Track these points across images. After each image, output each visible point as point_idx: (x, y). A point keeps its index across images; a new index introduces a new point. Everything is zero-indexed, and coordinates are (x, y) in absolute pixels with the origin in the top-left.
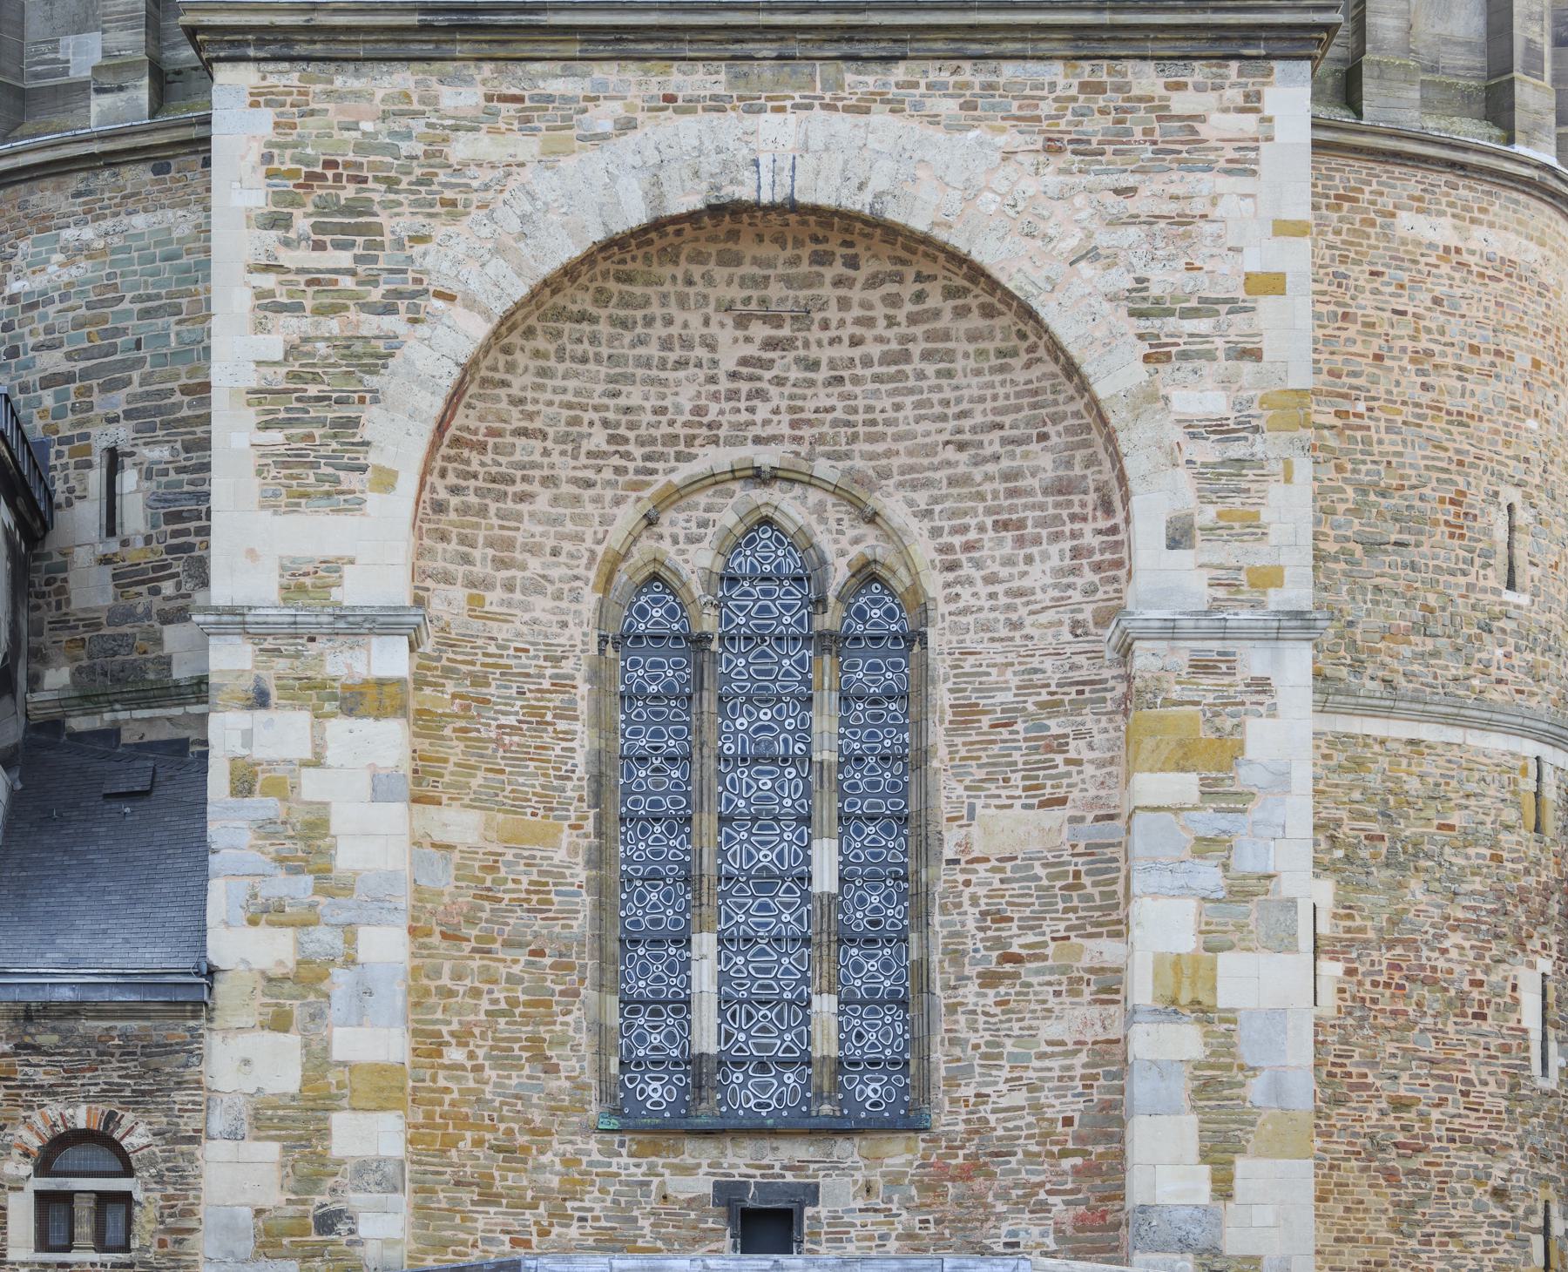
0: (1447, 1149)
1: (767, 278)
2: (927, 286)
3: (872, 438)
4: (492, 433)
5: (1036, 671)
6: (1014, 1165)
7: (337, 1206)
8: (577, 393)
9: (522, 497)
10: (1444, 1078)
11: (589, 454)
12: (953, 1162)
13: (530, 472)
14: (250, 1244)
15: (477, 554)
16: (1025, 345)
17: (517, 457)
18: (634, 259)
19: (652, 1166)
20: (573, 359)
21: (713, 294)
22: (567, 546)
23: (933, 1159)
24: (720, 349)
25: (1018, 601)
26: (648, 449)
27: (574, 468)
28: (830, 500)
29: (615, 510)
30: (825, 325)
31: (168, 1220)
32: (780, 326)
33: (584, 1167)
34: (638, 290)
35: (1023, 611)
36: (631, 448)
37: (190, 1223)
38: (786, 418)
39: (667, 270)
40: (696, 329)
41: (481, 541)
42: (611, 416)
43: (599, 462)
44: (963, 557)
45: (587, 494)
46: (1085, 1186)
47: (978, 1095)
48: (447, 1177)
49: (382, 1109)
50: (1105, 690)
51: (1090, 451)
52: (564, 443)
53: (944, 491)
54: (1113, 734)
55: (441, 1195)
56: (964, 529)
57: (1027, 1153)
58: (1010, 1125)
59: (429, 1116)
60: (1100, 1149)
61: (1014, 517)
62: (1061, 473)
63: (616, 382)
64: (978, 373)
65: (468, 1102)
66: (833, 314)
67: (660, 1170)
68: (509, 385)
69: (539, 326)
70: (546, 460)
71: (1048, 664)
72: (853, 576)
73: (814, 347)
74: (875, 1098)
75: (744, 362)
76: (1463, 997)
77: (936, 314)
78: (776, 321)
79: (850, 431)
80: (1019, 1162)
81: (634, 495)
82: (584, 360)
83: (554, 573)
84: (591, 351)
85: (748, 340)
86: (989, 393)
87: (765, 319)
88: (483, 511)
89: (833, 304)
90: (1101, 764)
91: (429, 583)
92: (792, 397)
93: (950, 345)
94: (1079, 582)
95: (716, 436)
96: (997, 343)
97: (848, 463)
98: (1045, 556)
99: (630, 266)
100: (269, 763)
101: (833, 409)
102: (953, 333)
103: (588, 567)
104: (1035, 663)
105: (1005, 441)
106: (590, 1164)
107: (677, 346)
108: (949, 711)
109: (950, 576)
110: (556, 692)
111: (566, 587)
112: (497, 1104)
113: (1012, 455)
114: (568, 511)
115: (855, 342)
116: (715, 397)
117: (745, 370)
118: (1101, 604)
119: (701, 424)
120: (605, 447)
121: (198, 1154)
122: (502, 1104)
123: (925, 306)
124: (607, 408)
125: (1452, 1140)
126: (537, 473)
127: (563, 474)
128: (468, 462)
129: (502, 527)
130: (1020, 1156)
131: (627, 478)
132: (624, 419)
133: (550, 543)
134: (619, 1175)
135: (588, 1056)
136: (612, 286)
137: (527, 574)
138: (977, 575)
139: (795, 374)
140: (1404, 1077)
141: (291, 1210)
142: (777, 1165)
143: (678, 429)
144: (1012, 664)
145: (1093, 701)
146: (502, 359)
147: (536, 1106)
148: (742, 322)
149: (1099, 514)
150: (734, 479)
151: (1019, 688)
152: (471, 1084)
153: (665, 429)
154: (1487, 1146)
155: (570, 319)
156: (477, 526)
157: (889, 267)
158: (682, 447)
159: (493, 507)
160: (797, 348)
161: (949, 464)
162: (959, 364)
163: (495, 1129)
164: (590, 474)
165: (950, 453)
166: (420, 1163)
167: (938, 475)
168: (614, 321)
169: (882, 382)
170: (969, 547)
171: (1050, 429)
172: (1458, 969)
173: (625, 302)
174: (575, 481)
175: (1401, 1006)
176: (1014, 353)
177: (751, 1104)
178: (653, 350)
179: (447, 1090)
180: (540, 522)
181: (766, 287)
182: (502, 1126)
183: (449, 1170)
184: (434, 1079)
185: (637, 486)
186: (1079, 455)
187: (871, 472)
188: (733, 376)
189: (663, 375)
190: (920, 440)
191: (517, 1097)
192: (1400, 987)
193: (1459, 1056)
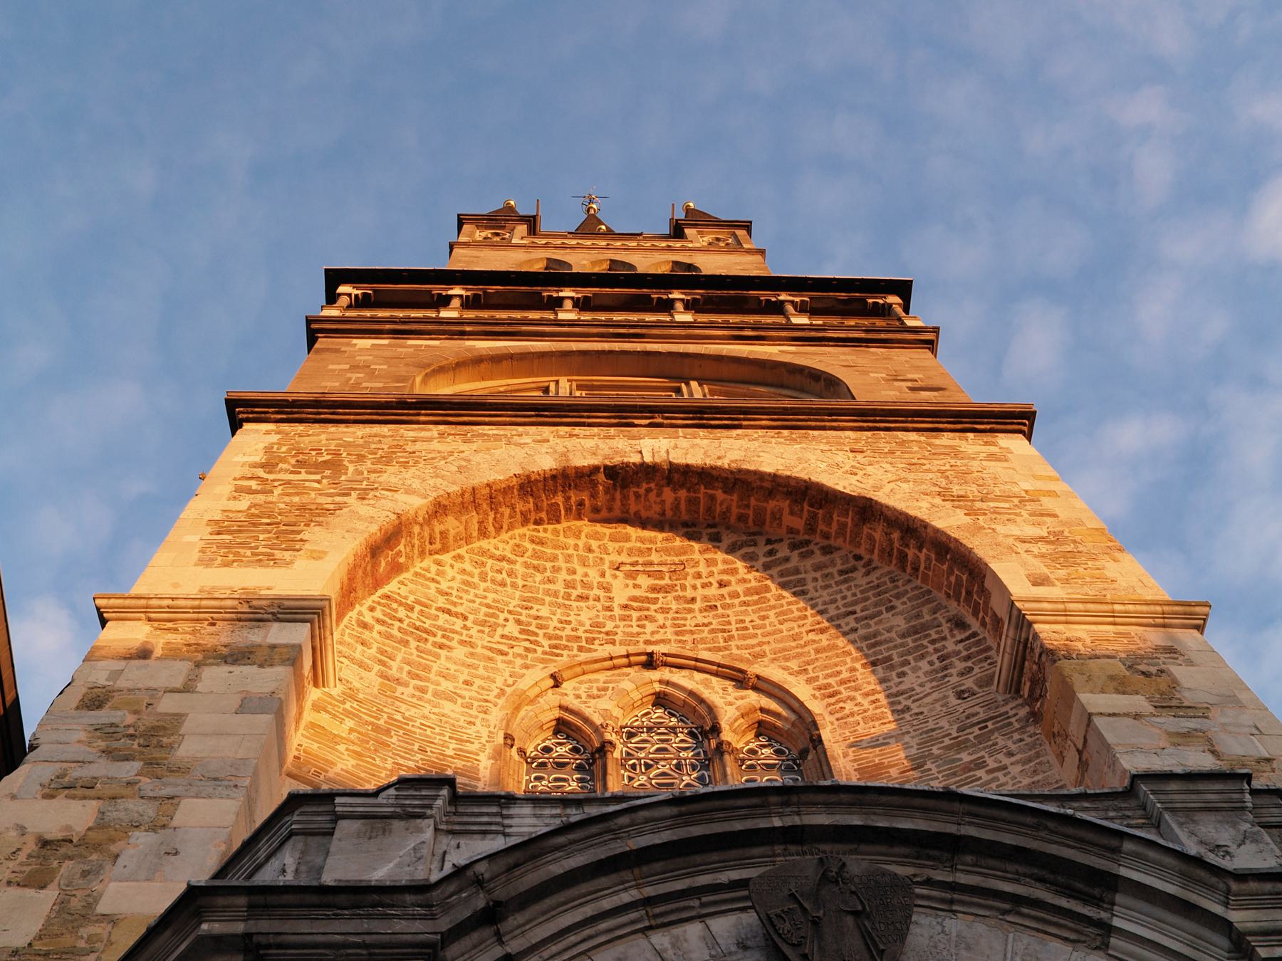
1: (649, 549)
2: (776, 546)
3: (744, 637)
4: (418, 602)
5: (933, 730)
8: (494, 601)
9: (441, 646)
11: (502, 636)
13: (451, 635)
15: (395, 665)
16: (862, 563)
17: (440, 622)
18: (545, 530)
20: (493, 581)
21: (607, 558)
22: (478, 682)
24: (614, 591)
25: (900, 698)
26: (554, 642)
27: (489, 642)
28: (714, 679)
29: (524, 671)
30: (699, 575)
32: (663, 578)
34: (549, 551)
35: (909, 703)
36: (540, 639)
38: (670, 630)
39: (571, 542)
40: (594, 576)
41: (399, 658)
42: (523, 618)
43: (511, 642)
44: (842, 688)
45: (500, 658)
50: (1009, 717)
51: (935, 604)
52: (483, 626)
53: (813, 657)
54: (1029, 740)
56: (839, 673)
61: (880, 657)
62: (912, 623)
63: (529, 601)
64: (826, 587)
66: (702, 568)
68: (438, 582)
69: (467, 556)
70: (465, 632)
71: (944, 723)
72: (743, 716)
73: (689, 589)
75: (634, 599)
77: (787, 559)
78: (659, 574)
79: (725, 635)
81: (542, 666)
82: (503, 584)
83: (467, 694)
84: (508, 581)
85: (635, 586)
86: (838, 597)
87: (649, 574)
88: (406, 643)
89: (702, 563)
90: (1025, 762)
91: (343, 659)
92: (674, 619)
93: (800, 576)
94: (954, 671)
95: (614, 639)
96: (839, 567)
97: (727, 652)
98: (915, 670)
99: (542, 534)
100: (129, 690)
101: (710, 623)
102: (802, 569)
103: (498, 696)
104: (931, 725)
105: (857, 620)
107: (579, 587)
108: (856, 773)
109: (832, 700)
110: (459, 759)
111: (476, 704)
113: (868, 626)
114: (482, 664)
115: (722, 584)
116: (612, 618)
117: (635, 604)
118: (979, 675)
119: (601, 632)
120: (516, 634)
123: (777, 557)
124: (521, 614)
126: (456, 637)
127: (479, 643)
128: (396, 611)
129: (418, 656)
131: (535, 655)
132: (534, 622)
133: (462, 678)
136: (527, 545)
137: (438, 688)
138: (857, 694)
139: (674, 606)
143: (580, 633)
144: (908, 732)
145: (998, 729)
146: (434, 568)
148: (631, 575)
149: (956, 632)
150: (630, 665)
151: (918, 744)
153: (568, 632)
155: (492, 557)
156: (397, 649)
157: (744, 538)
158: (584, 644)
159: (413, 644)
160: (676, 591)
161: (814, 641)
162: (810, 586)
164: (504, 648)
165: (812, 636)
167: (806, 649)
168: (526, 565)
169: (749, 605)
170: (842, 682)
171: (895, 602)
173: (536, 555)
174: (490, 649)
176: (854, 569)
178: (559, 586)
180: (455, 663)
181: (650, 555)
185: (542, 661)
186: (925, 610)
187: (748, 656)
188: (625, 607)
189: (567, 602)
190: (785, 633)
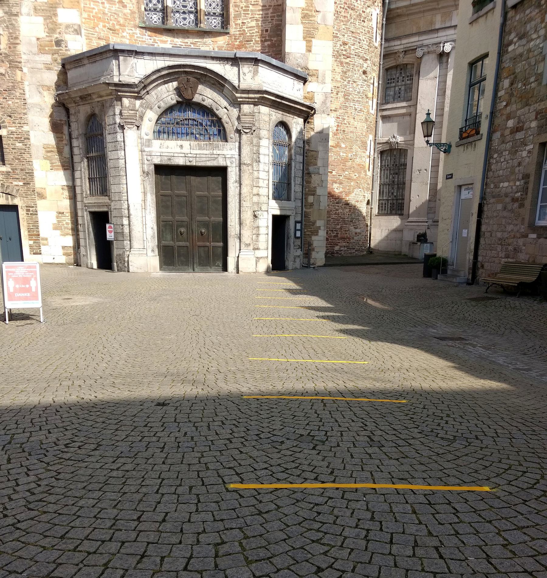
0: (354, 58)
6: (252, 45)
7: (61, 38)
10: (355, 37)
12: (236, 43)
14: (36, 49)
19: (155, 40)
23: (231, 42)
31: (11, 40)
33: (135, 38)
37: (18, 41)
46: (271, 51)
47: (243, 23)
48: (95, 36)
49: (72, 8)
55: (94, 41)
57: (255, 40)
58: (251, 32)
59: (89, 16)
60: (275, 39)
65: (100, 13)
67: (157, 41)
74: (215, 24)
76: (360, 15)
80: (254, 44)
106: (137, 37)
112: (109, 15)
121: (19, 20)
122: (111, 15)
125: (356, 55)
130: (254, 41)
134: (145, 41)
135: (135, 4)
140: (346, 36)
141: (48, 39)
142: (189, 42)
147: (121, 17)
152: (101, 8)
154: (362, 58)
163: (109, 23)
166: (87, 30)
172: (360, 7)
175: (346, 15)
177: (182, 24)
179: (94, 8)
182: (111, 22)
183: (96, 34)
184: (90, 4)
191: (115, 13)
192: (346, 9)
193: (358, 32)
